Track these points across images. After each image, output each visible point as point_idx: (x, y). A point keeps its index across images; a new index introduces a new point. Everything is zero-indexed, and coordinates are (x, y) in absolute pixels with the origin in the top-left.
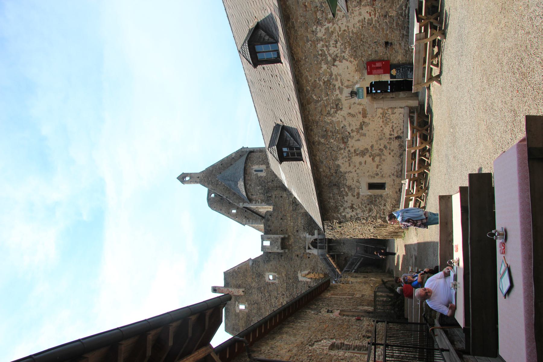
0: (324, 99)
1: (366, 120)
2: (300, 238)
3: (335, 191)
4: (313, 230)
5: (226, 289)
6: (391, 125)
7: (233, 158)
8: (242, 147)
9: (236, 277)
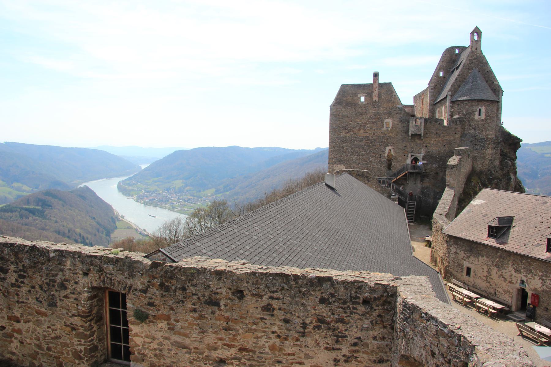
0: (522, 266)
1: (507, 282)
2: (421, 149)
3: (467, 248)
4: (427, 160)
5: (377, 85)
6: (503, 293)
7: (493, 82)
8: (503, 90)
9: (387, 93)
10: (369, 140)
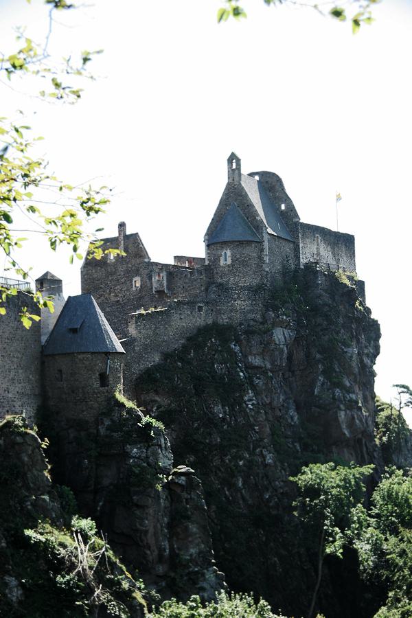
5: (122, 238)
10: (120, 304)
